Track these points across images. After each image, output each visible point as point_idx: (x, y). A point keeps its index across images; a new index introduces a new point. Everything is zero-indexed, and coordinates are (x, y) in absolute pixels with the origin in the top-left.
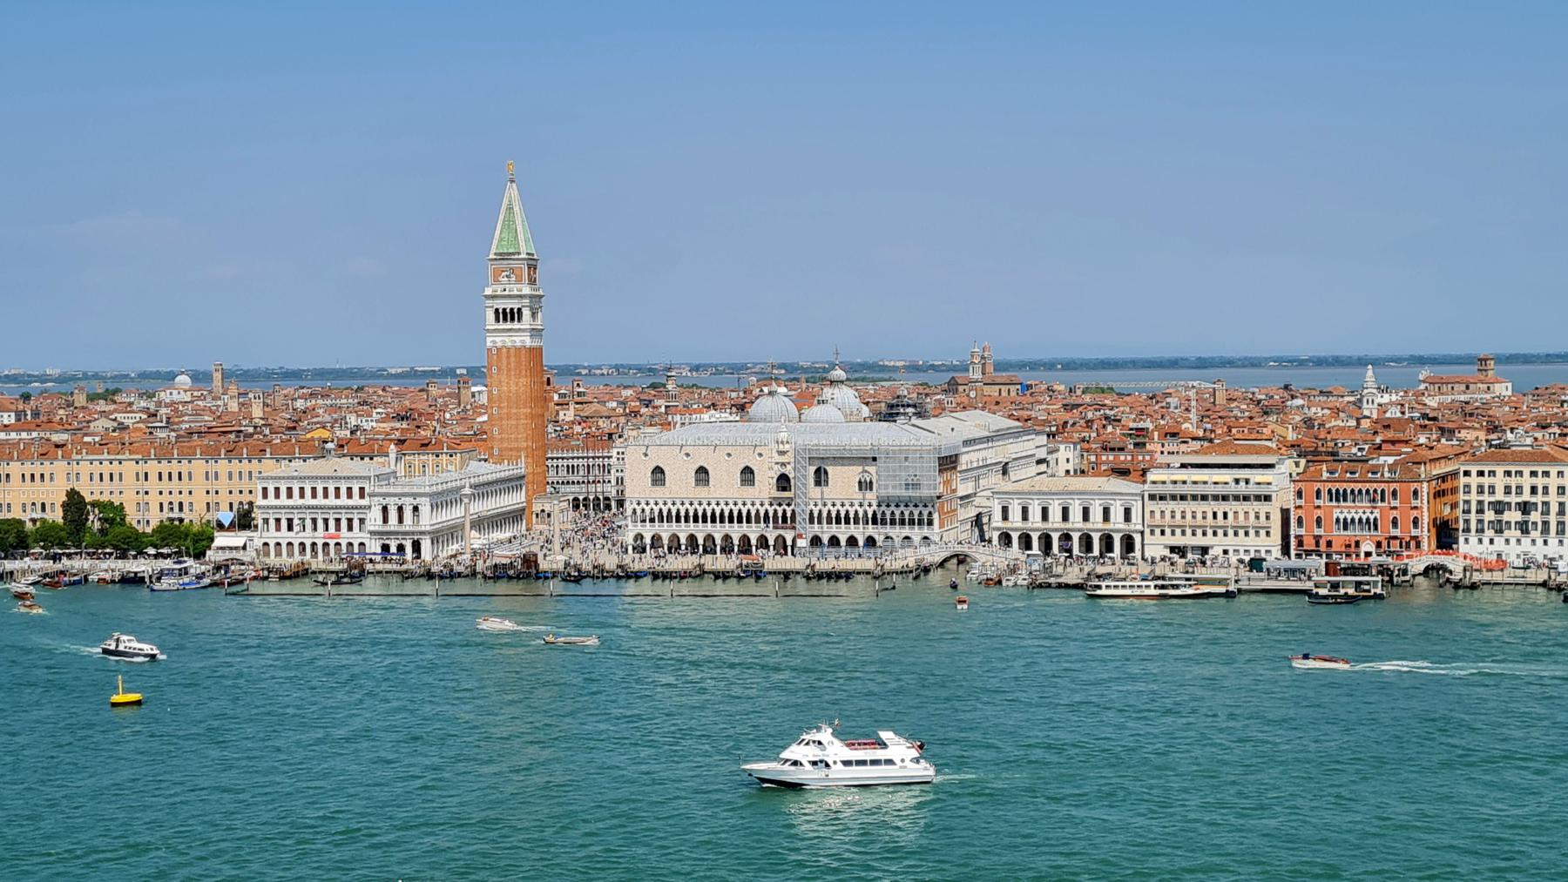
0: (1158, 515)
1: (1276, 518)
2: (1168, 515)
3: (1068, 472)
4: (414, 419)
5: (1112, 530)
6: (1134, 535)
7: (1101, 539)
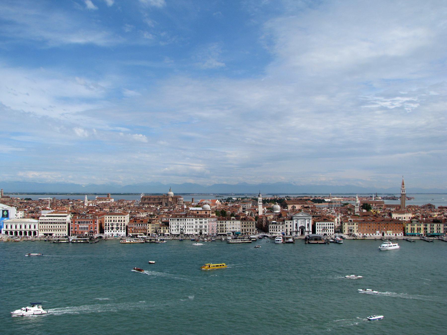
0: (41, 227)
1: (67, 227)
2: (44, 227)
3: (21, 217)
5: (22, 230)
6: (36, 231)
7: (29, 232)
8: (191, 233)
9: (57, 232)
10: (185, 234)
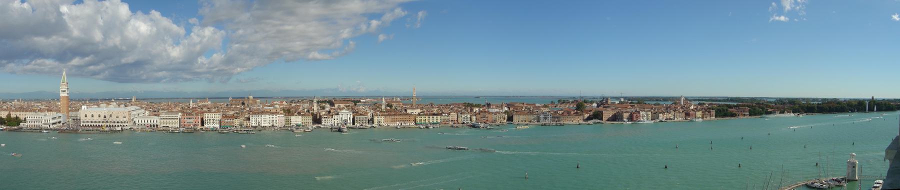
1: (179, 121)
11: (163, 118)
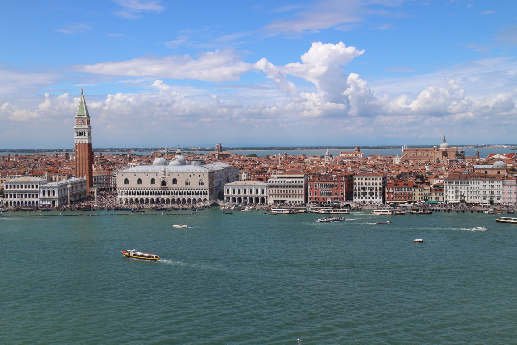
0: (271, 192)
2: (274, 192)
4: (52, 165)
8: (476, 201)
9: (291, 199)
10: (468, 203)
11: (274, 184)
